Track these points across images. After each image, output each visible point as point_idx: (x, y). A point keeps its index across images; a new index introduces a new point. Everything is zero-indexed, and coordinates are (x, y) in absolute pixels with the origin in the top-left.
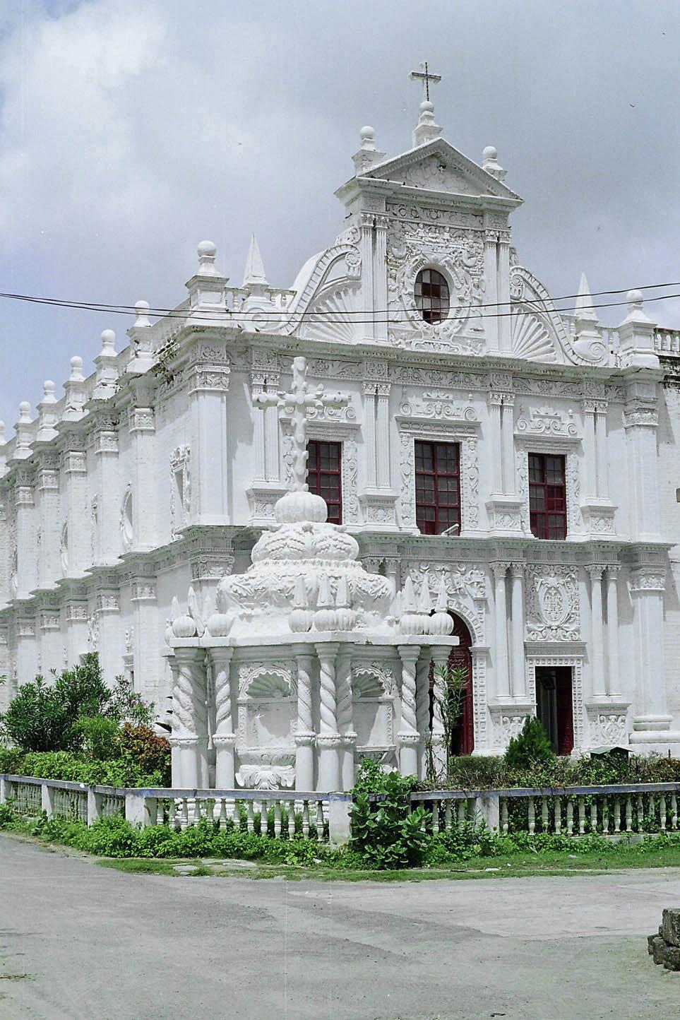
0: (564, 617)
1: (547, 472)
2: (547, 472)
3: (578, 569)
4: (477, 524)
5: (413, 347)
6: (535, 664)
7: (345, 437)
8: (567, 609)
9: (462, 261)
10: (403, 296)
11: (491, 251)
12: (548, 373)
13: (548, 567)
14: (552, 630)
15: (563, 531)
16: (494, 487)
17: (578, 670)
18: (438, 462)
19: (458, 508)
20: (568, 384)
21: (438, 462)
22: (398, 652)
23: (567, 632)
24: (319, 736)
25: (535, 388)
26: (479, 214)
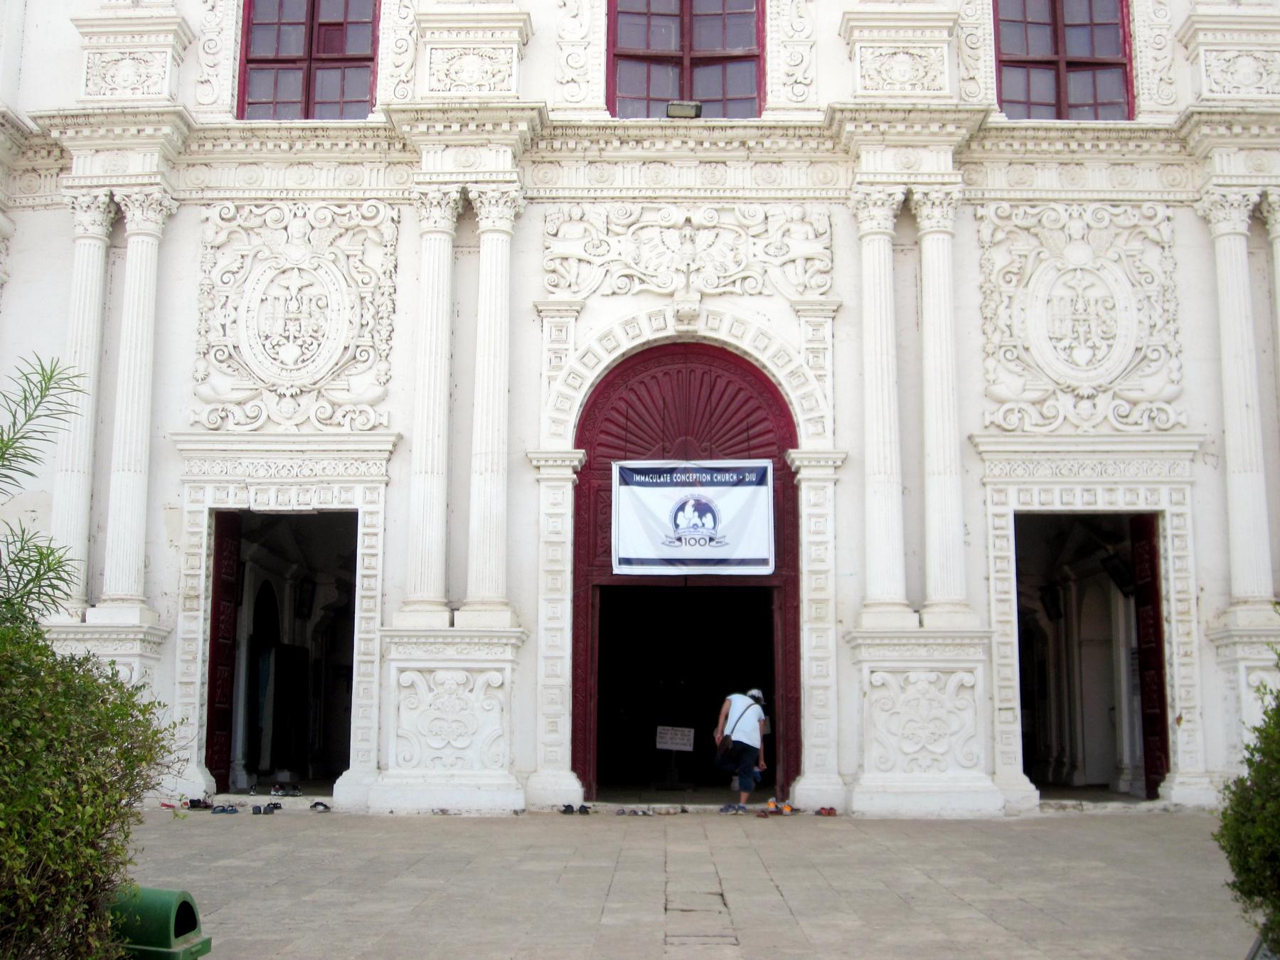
0: (1121, 353)
3: (1169, 212)
6: (1016, 503)
13: (1060, 208)
17: (1176, 521)
23: (1134, 403)
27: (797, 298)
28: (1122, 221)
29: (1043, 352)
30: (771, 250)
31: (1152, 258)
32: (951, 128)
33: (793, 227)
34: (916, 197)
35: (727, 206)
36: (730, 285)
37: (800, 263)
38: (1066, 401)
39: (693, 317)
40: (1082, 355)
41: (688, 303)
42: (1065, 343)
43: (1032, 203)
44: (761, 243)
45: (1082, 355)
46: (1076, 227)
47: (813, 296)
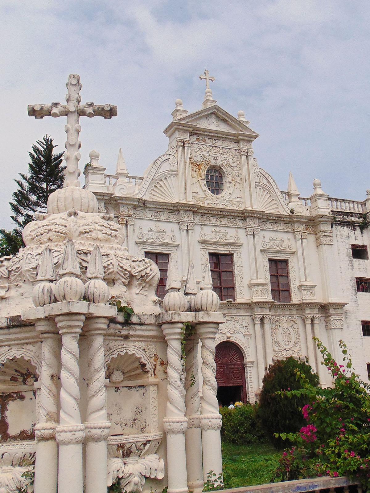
0: (292, 343)
1: (279, 267)
2: (279, 267)
4: (243, 295)
5: (206, 204)
7: (171, 251)
8: (293, 339)
9: (229, 164)
10: (200, 180)
11: (244, 159)
12: (276, 218)
13: (282, 317)
14: (287, 351)
15: (289, 298)
16: (251, 276)
18: (221, 264)
19: (233, 288)
20: (286, 225)
21: (221, 264)
22: (162, 331)
23: (295, 351)
24: (59, 428)
25: (270, 226)
26: (237, 141)
27: (244, 334)
28: (291, 319)
29: (282, 343)
30: (240, 325)
31: (295, 326)
32: (269, 305)
33: (243, 321)
34: (264, 317)
35: (233, 317)
36: (237, 332)
37: (244, 327)
38: (285, 351)
39: (229, 338)
40: (287, 343)
41: (229, 335)
42: (284, 341)
43: (278, 316)
44: (238, 323)
45: (287, 343)
46: (285, 320)
47: (247, 333)
